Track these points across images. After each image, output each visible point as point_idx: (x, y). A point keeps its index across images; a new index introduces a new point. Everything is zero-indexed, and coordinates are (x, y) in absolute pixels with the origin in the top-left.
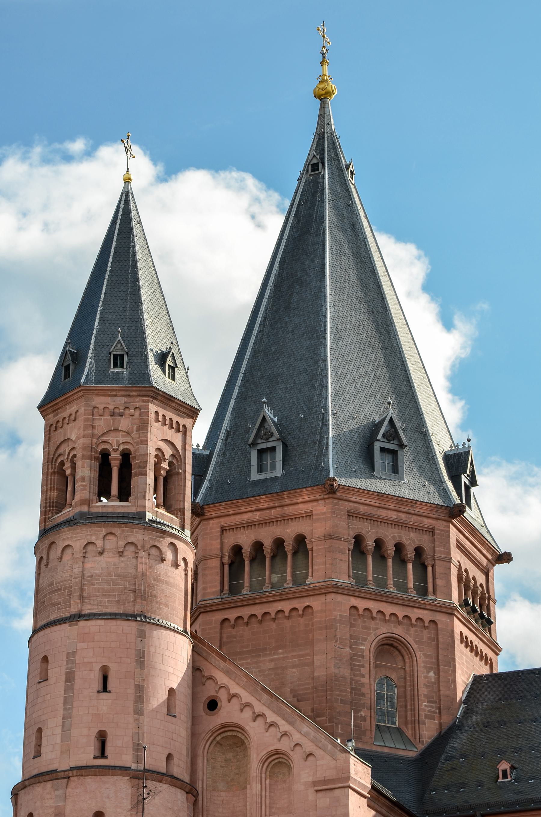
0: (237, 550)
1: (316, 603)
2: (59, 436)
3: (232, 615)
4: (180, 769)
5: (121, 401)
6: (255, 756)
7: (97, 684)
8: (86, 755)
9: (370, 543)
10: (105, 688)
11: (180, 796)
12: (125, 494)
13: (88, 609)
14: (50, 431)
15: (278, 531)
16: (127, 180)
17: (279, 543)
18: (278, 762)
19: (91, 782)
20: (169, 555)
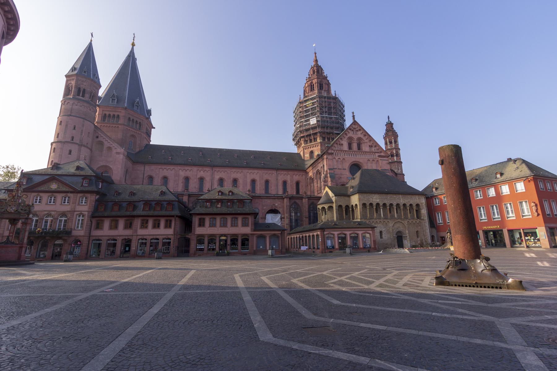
0: (105, 114)
1: (120, 126)
2: (69, 82)
3: (103, 125)
4: (89, 146)
5: (84, 79)
6: (105, 147)
7: (73, 127)
8: (69, 140)
9: (131, 119)
10: (74, 128)
11: (89, 150)
12: (83, 96)
13: (72, 114)
14: (67, 81)
15: (114, 113)
16: (91, 41)
17: (114, 115)
18: (110, 149)
20: (92, 110)
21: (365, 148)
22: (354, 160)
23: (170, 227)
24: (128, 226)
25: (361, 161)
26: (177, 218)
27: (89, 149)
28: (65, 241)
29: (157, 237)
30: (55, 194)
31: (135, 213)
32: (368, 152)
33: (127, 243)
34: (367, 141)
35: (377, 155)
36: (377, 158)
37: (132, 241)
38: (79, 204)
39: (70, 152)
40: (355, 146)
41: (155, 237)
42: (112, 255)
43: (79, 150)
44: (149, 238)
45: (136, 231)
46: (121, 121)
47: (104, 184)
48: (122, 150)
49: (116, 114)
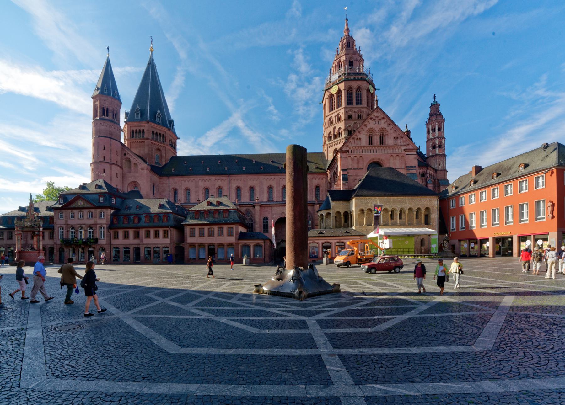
0: (133, 130)
1: (146, 141)
3: (132, 141)
4: (119, 164)
18: (136, 164)
19: (102, 164)
21: (389, 141)
22: (374, 157)
23: (168, 237)
24: (137, 236)
25: (382, 158)
26: (172, 229)
27: (119, 166)
28: (94, 248)
29: (158, 246)
30: (83, 210)
31: (139, 225)
32: (392, 146)
33: (137, 250)
34: (392, 131)
35: (403, 148)
36: (403, 152)
37: (141, 249)
38: (99, 218)
39: (104, 170)
40: (376, 139)
41: (156, 246)
42: (126, 261)
43: (111, 168)
44: (152, 246)
45: (142, 240)
46: (147, 135)
47: (119, 200)
48: (144, 165)
49: (141, 128)
